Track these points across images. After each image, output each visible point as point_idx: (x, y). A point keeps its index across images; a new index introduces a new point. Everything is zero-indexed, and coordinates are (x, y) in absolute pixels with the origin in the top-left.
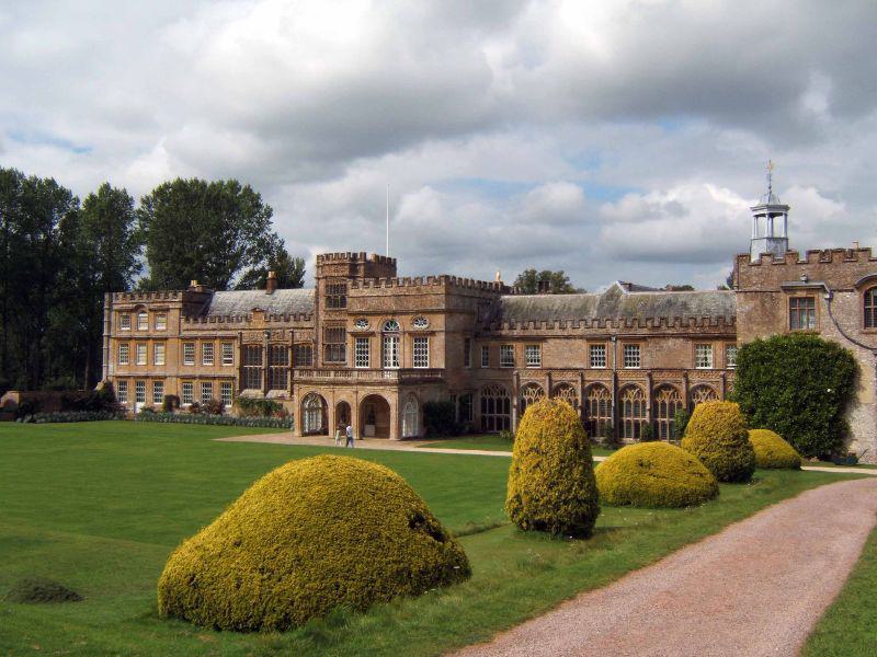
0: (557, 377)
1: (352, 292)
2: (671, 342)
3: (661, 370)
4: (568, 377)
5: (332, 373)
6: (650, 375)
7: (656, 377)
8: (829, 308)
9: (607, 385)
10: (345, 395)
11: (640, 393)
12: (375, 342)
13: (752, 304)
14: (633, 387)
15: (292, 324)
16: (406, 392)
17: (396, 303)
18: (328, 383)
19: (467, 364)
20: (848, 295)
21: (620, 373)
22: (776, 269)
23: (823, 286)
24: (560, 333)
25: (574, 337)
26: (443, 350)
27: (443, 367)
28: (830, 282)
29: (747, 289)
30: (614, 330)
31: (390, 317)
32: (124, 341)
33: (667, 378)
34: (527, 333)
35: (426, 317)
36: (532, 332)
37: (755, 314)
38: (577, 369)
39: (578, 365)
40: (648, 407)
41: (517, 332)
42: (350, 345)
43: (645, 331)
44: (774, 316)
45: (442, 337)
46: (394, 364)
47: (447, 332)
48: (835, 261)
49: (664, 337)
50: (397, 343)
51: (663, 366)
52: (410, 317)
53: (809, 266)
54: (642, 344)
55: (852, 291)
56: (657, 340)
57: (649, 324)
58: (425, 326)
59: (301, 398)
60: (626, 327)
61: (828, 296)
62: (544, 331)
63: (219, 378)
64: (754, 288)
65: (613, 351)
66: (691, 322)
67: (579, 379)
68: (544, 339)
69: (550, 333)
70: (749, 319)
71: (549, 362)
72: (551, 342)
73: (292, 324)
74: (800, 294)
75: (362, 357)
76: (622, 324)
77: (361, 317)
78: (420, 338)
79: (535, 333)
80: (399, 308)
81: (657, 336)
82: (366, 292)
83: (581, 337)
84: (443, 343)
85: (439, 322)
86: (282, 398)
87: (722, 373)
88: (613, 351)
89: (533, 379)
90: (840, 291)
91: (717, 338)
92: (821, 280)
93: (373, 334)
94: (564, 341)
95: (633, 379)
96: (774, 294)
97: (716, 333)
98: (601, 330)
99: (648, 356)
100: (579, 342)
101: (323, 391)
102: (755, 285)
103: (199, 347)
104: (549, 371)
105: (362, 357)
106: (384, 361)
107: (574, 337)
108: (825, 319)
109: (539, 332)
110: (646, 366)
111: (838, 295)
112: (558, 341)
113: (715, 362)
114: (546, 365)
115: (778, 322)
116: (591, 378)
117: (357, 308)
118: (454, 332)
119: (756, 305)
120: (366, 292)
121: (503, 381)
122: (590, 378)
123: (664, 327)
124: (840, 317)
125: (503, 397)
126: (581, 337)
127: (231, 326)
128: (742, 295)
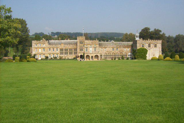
7: (120, 52)
10: (92, 55)
15: (68, 45)
32: (36, 48)
33: (121, 52)
62: (107, 47)
63: (56, 53)
65: (115, 49)
68: (106, 47)
73: (68, 45)
75: (87, 50)
77: (87, 45)
78: (95, 48)
81: (120, 47)
88: (115, 49)
95: (117, 52)
99: (119, 49)
103: (52, 49)
105: (87, 50)
116: (113, 52)
127: (57, 46)
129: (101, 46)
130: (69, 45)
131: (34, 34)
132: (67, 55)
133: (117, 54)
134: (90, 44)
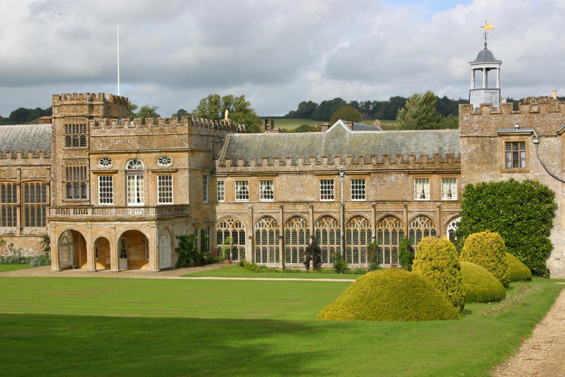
0: (289, 209)
1: (94, 132)
2: (393, 177)
3: (384, 202)
4: (300, 208)
5: (90, 211)
6: (374, 206)
7: (380, 208)
8: (537, 151)
9: (335, 216)
11: (367, 222)
12: (118, 180)
13: (474, 147)
14: (359, 217)
15: (20, 161)
16: (162, 227)
17: (139, 143)
18: (86, 221)
19: (205, 199)
20: (552, 140)
21: (347, 205)
22: (494, 117)
23: (532, 132)
24: (292, 169)
25: (305, 172)
26: (187, 187)
27: (187, 202)
28: (538, 129)
29: (470, 134)
30: (341, 167)
31: (134, 156)
33: (390, 208)
34: (261, 169)
35: (170, 155)
36: (265, 168)
37: (476, 156)
38: (307, 202)
39: (310, 199)
40: (373, 235)
41: (252, 168)
42: (95, 183)
43: (370, 167)
44: (492, 157)
45: (186, 174)
46: (139, 201)
47: (191, 170)
48: (542, 111)
49: (388, 172)
50: (140, 181)
51: (386, 199)
52: (155, 155)
53: (521, 115)
54: (367, 179)
55: (556, 136)
56: (381, 175)
57: (374, 161)
58: (169, 165)
59: (57, 236)
60: (353, 164)
61: (536, 141)
62: (277, 167)
64: (476, 134)
66: (411, 159)
67: (310, 210)
68: (276, 174)
69: (282, 169)
70: (472, 160)
71: (281, 196)
72: (284, 177)
73: (20, 161)
74: (513, 139)
75: (106, 194)
76: (349, 161)
79: (268, 169)
80: (142, 147)
81: (380, 171)
82: (108, 132)
83: (312, 172)
84: (187, 181)
85: (183, 160)
86: (11, 235)
87: (438, 204)
89: (267, 212)
90: (547, 136)
91: (434, 173)
92: (530, 127)
93: (116, 172)
94: (296, 177)
95: (359, 209)
96: (492, 139)
97: (432, 168)
98: (330, 167)
100: (310, 177)
101: (80, 227)
102: (475, 131)
104: (282, 204)
105: (106, 194)
106: (127, 195)
107: (305, 172)
108: (533, 161)
109: (272, 169)
110: (371, 199)
111: (544, 140)
112: (290, 177)
113: (431, 194)
114: (279, 199)
115: (496, 162)
116: (323, 209)
117: (99, 146)
118: (195, 170)
119: (477, 149)
120: (108, 132)
121: (239, 214)
122: (320, 210)
123: (387, 163)
124: (546, 158)
125: (238, 229)
126: (312, 172)
128: (466, 139)
129: (234, 165)
130: (24, 157)
131: (296, 109)
132: (9, 229)
133: (358, 226)
134: (129, 148)
